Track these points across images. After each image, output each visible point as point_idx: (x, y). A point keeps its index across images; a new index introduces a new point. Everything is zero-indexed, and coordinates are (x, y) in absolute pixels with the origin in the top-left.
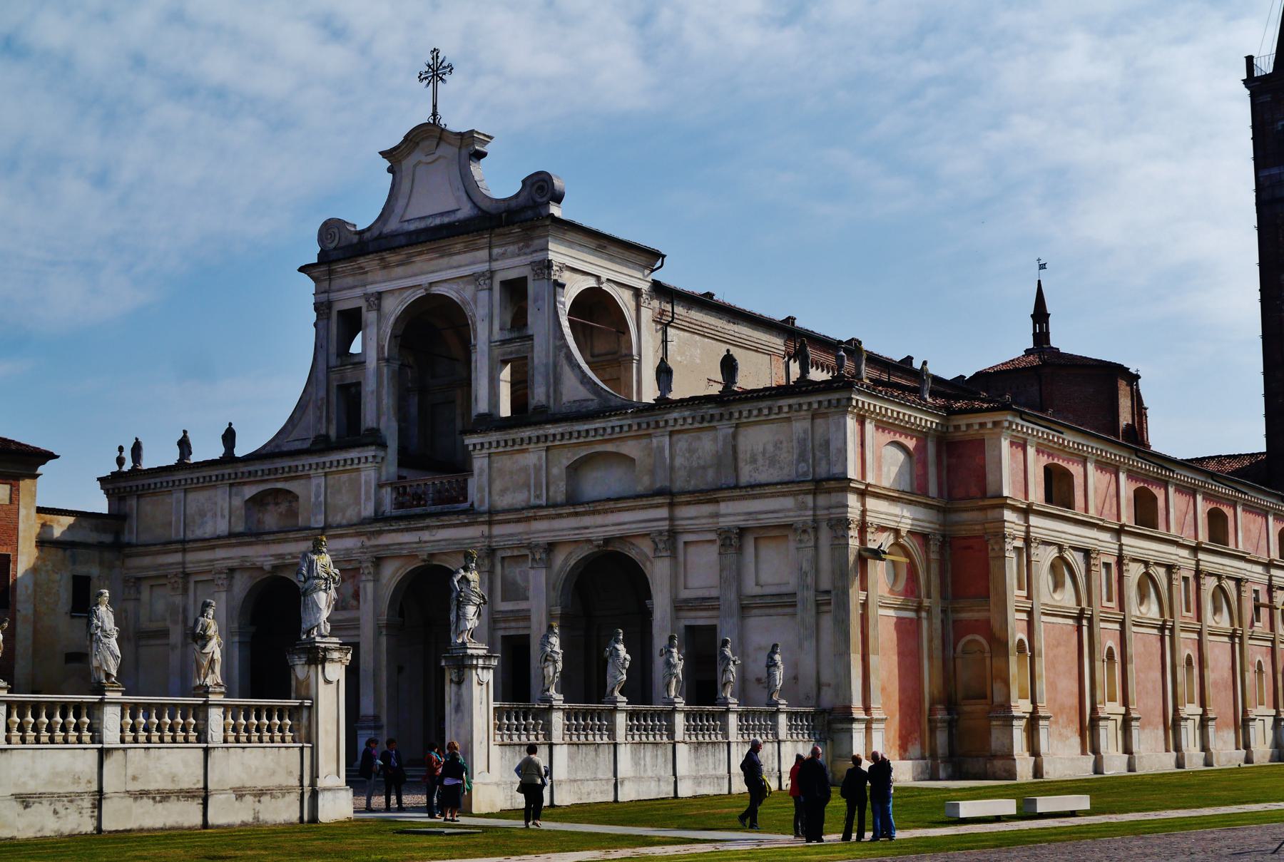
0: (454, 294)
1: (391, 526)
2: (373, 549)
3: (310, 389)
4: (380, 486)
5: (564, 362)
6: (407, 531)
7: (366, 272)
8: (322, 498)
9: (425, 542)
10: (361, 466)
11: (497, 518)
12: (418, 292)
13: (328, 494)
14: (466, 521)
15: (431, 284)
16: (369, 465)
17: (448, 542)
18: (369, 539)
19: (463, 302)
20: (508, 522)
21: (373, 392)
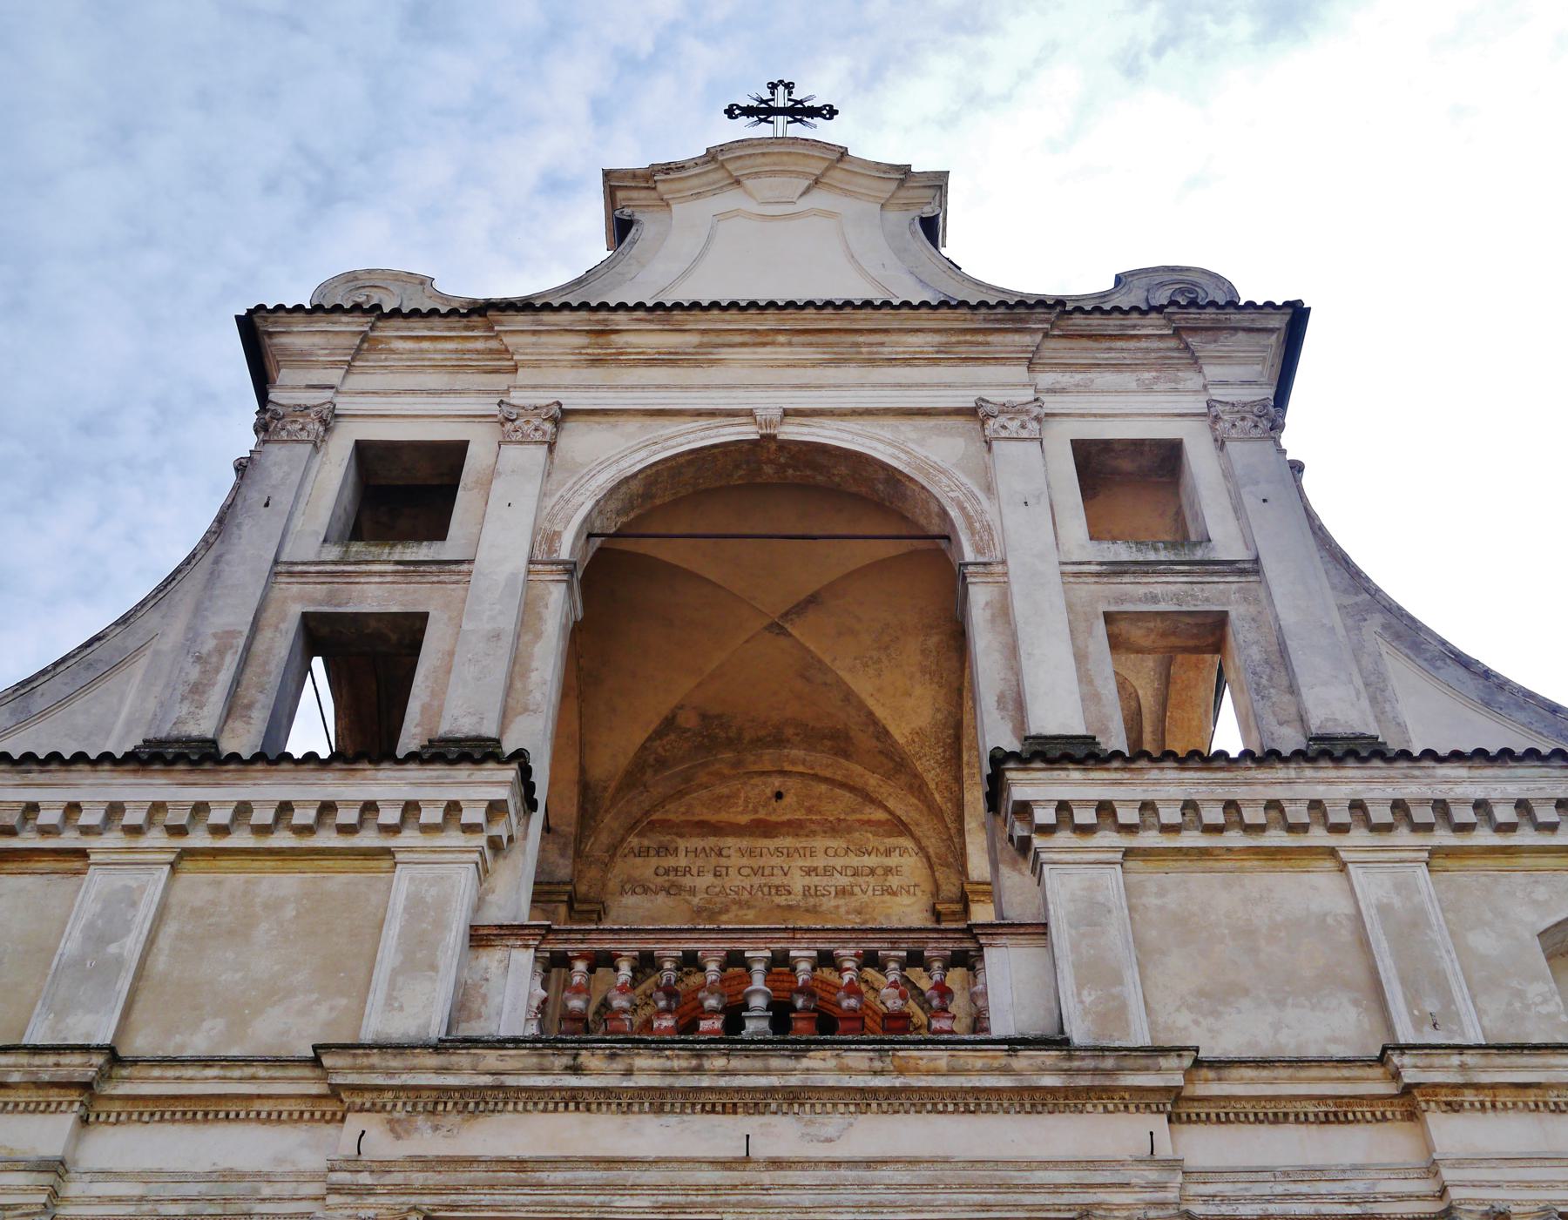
0: (880, 446)
1: (576, 1070)
2: (418, 1178)
3: (152, 620)
4: (479, 938)
5: (1384, 649)
6: (659, 1110)
7: (515, 369)
8: (131, 946)
9: (776, 1164)
10: (409, 838)
11: (1215, 1089)
12: (722, 431)
13: (164, 942)
14: (1049, 1081)
15: (786, 413)
16: (454, 838)
17: (924, 1174)
18: (396, 1130)
19: (920, 469)
20: (1273, 1113)
21: (497, 636)
